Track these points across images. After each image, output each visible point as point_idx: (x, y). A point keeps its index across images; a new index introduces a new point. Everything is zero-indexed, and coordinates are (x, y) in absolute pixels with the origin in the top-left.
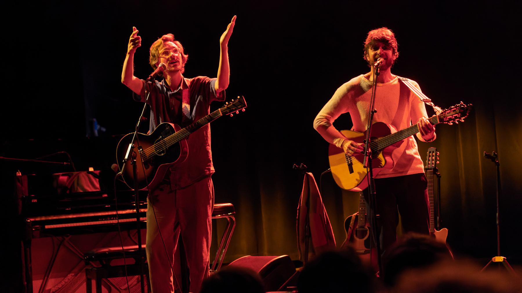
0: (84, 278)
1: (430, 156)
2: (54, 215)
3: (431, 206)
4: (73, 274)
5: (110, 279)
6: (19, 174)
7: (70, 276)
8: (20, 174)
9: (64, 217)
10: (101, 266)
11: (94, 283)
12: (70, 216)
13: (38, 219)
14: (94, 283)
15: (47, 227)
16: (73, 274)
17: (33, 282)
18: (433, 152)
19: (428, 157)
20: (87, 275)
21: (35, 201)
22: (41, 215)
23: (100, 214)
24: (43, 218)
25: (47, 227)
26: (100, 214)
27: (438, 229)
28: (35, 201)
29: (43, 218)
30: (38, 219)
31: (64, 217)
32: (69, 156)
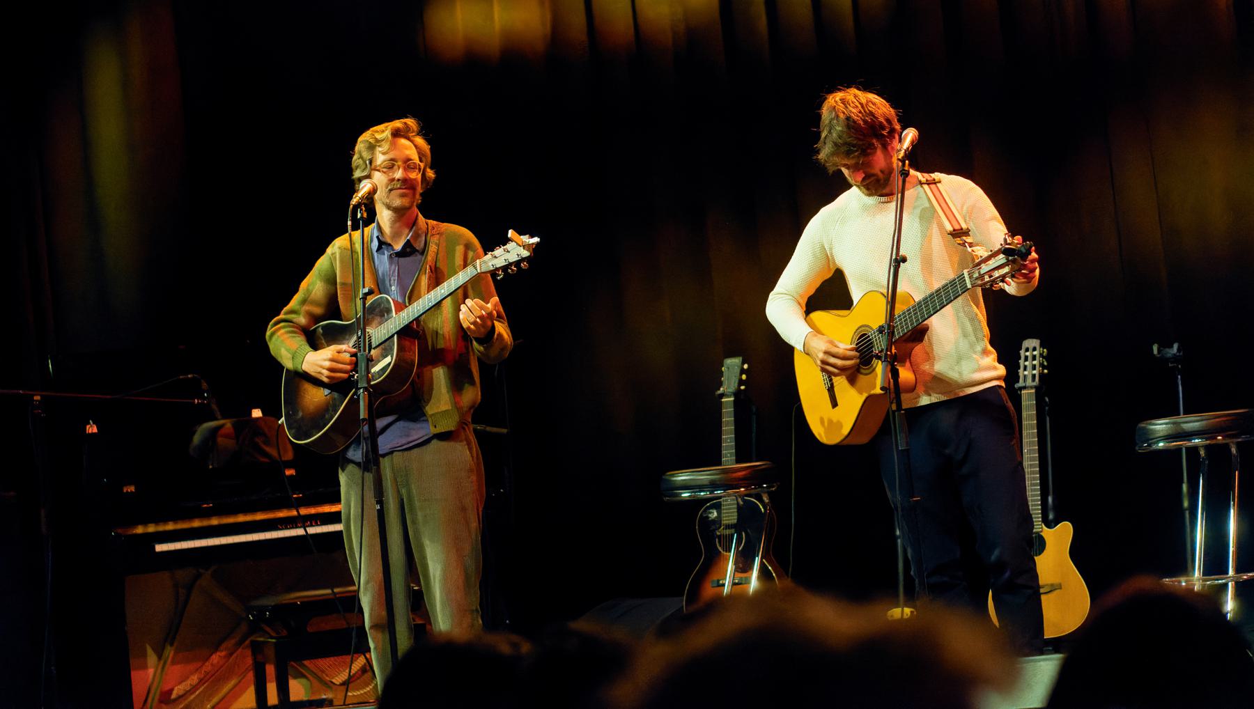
0: (249, 661)
1: (1026, 359)
2: (175, 519)
3: (1033, 473)
4: (223, 654)
5: (306, 663)
6: (92, 429)
7: (215, 658)
8: (95, 430)
9: (196, 524)
10: (285, 633)
11: (270, 670)
12: (215, 521)
13: (140, 530)
14: (270, 670)
15: (160, 548)
16: (223, 654)
17: (133, 673)
18: (1034, 349)
19: (1021, 362)
20: (254, 654)
21: (132, 489)
22: (145, 523)
23: (282, 514)
24: (151, 529)
25: (160, 548)
26: (282, 514)
27: (1050, 524)
28: (132, 489)
29: (151, 529)
30: (140, 530)
31: (196, 524)
32: (205, 385)
